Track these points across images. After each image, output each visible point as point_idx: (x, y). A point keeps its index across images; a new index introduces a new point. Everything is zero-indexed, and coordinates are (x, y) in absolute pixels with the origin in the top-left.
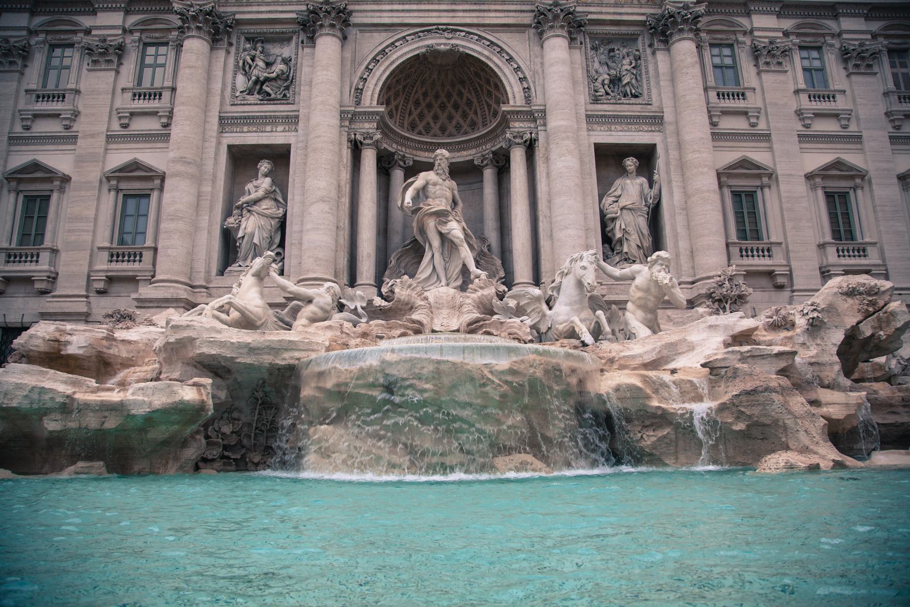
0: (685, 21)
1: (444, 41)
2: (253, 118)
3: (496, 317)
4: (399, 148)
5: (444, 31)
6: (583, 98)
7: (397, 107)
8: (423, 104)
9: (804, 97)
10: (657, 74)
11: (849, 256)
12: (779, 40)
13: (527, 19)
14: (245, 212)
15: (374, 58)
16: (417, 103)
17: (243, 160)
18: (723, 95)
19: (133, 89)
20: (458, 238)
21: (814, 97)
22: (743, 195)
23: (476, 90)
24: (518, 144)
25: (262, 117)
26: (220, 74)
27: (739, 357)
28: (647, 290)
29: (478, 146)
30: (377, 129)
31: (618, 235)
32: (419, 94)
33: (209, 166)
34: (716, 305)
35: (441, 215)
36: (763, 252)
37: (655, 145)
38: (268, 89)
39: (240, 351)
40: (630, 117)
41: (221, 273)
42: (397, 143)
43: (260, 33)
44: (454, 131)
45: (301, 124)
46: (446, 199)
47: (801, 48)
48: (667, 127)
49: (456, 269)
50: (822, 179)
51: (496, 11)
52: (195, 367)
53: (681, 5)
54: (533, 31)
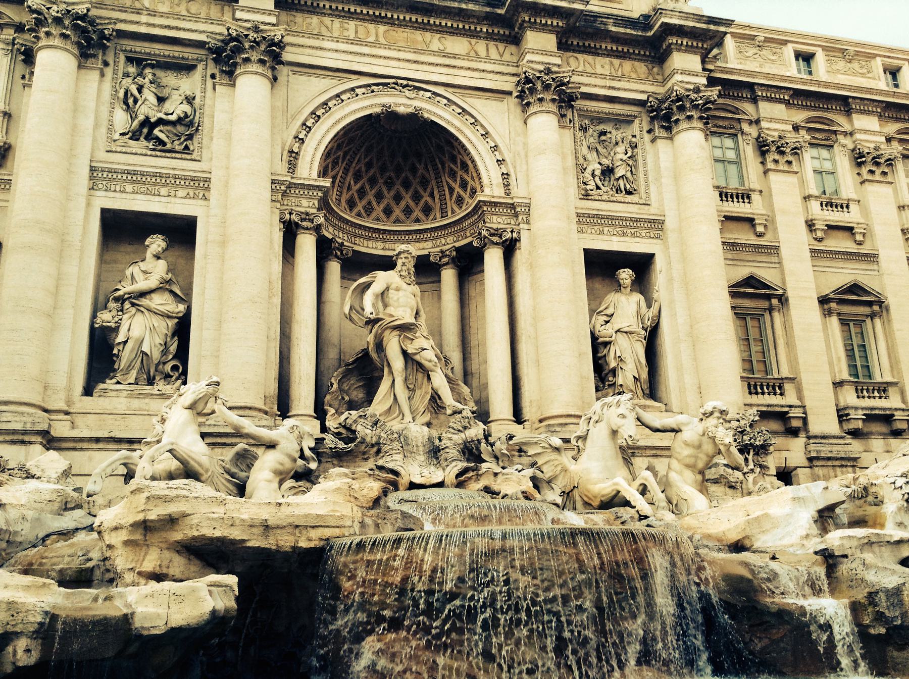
0: (696, 107)
1: (404, 101)
2: (142, 174)
3: (484, 465)
5: (404, 87)
6: (573, 192)
8: (365, 179)
9: (815, 205)
10: (658, 168)
11: (869, 397)
12: (788, 135)
13: (508, 84)
14: (127, 305)
15: (313, 113)
16: (357, 177)
17: (122, 230)
18: (726, 196)
20: (430, 361)
22: (748, 319)
23: (436, 169)
24: (497, 244)
25: (155, 175)
26: (92, 105)
27: (855, 543)
28: (699, 447)
29: (437, 238)
30: (318, 210)
31: (613, 364)
33: (76, 234)
36: (774, 387)
37: (652, 256)
38: (162, 136)
39: (255, 530)
41: (88, 391)
43: (149, 54)
44: (402, 217)
45: (214, 194)
46: (412, 310)
47: (812, 145)
48: (669, 232)
49: (422, 399)
50: (838, 303)
51: (469, 69)
52: (178, 552)
53: (692, 87)
54: (512, 101)
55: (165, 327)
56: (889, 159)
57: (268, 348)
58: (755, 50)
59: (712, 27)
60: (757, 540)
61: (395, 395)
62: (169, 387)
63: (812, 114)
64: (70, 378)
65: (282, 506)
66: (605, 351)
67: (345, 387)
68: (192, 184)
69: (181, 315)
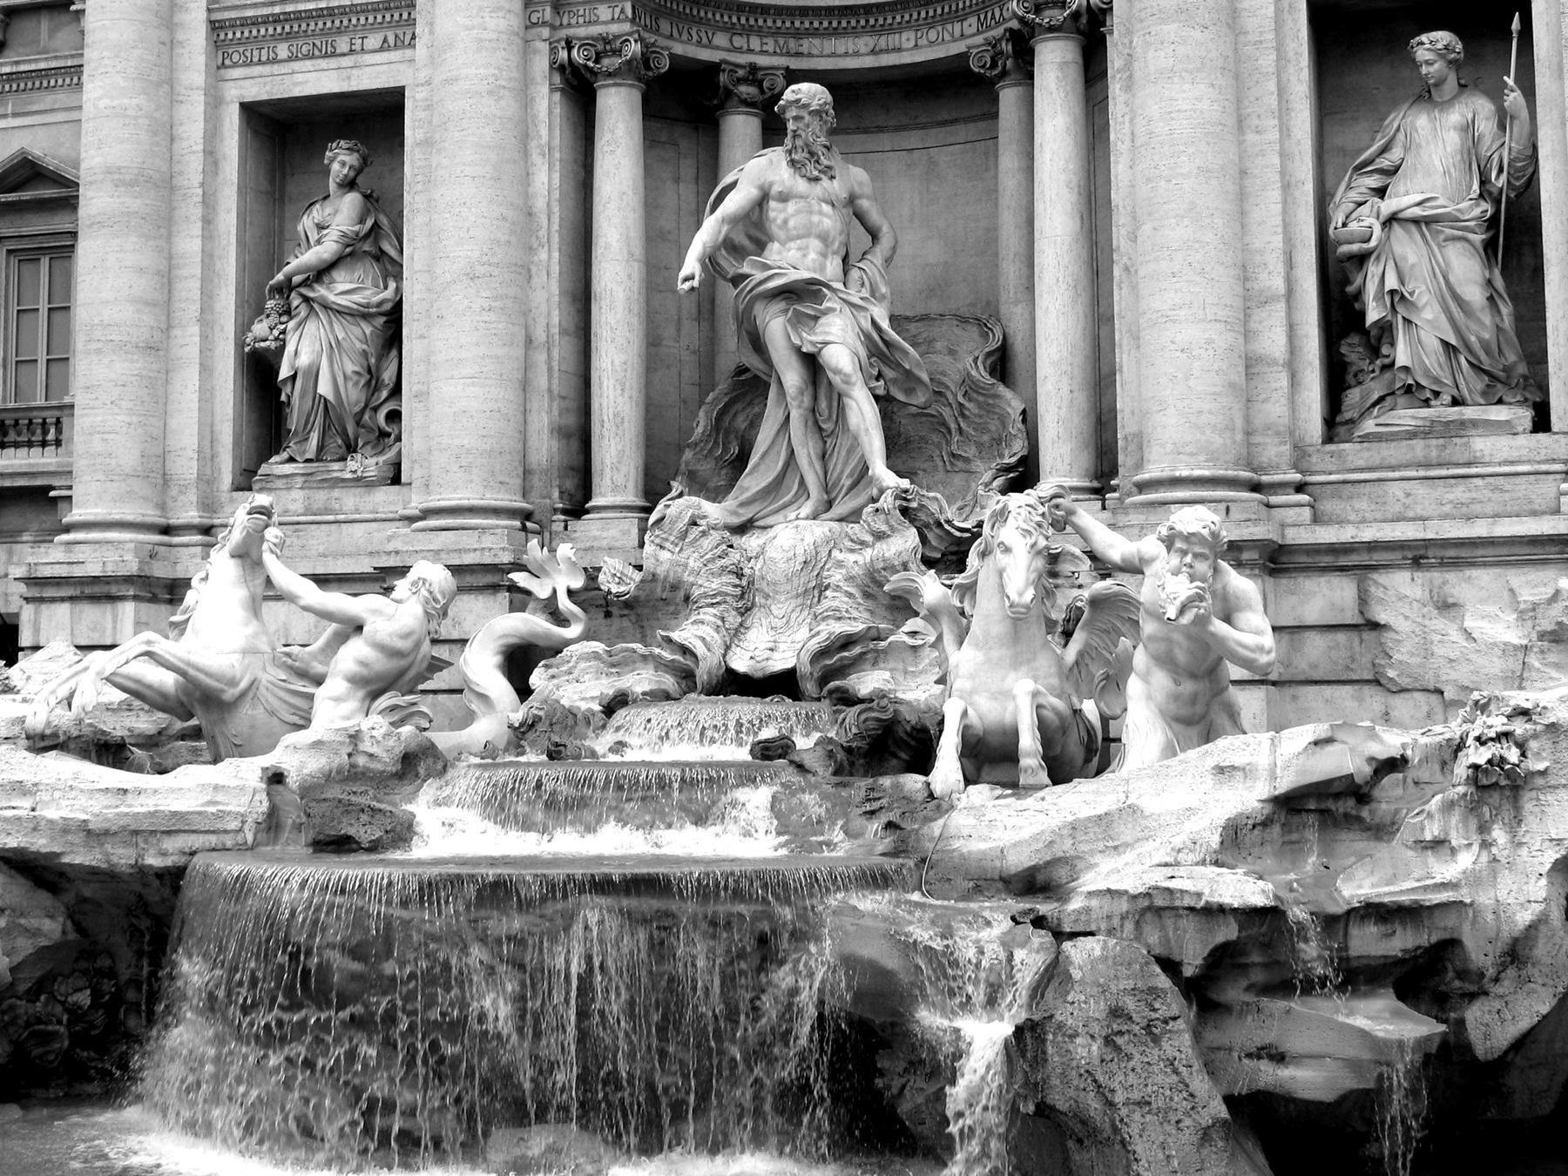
3: (912, 624)
4: (739, 41)
17: (286, 138)
20: (837, 372)
27: (1124, 906)
30: (633, 21)
31: (1373, 314)
41: (246, 481)
42: (730, 29)
46: (824, 238)
55: (358, 336)
57: (527, 367)
60: (1091, 866)
62: (373, 461)
64: (207, 456)
65: (129, 796)
66: (1359, 281)
67: (741, 423)
68: (388, 18)
69: (387, 307)
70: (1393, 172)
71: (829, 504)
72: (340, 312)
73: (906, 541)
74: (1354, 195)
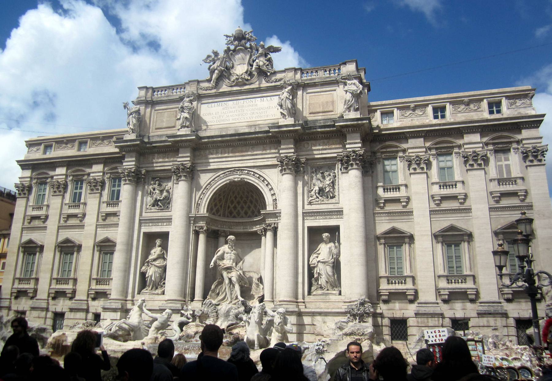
1: (238, 176)
2: (153, 219)
5: (238, 170)
7: (221, 206)
9: (436, 187)
11: (455, 283)
16: (232, 202)
18: (387, 189)
19: (107, 202)
21: (443, 186)
30: (206, 224)
31: (315, 276)
32: (233, 198)
34: (352, 318)
35: (229, 269)
40: (326, 212)
46: (233, 260)
47: (439, 155)
55: (159, 271)
56: (483, 156)
58: (411, 112)
59: (360, 122)
61: (226, 294)
63: (438, 140)
70: (319, 254)
71: (231, 302)
72: (157, 266)
73: (242, 309)
74: (313, 257)
